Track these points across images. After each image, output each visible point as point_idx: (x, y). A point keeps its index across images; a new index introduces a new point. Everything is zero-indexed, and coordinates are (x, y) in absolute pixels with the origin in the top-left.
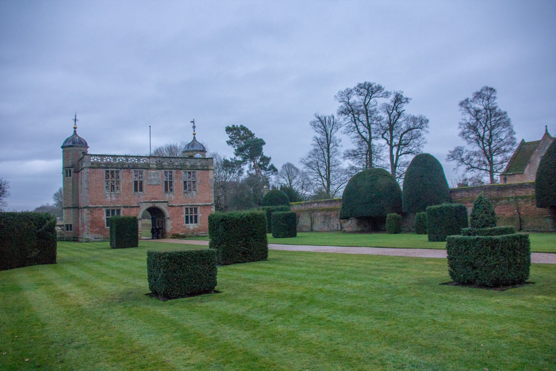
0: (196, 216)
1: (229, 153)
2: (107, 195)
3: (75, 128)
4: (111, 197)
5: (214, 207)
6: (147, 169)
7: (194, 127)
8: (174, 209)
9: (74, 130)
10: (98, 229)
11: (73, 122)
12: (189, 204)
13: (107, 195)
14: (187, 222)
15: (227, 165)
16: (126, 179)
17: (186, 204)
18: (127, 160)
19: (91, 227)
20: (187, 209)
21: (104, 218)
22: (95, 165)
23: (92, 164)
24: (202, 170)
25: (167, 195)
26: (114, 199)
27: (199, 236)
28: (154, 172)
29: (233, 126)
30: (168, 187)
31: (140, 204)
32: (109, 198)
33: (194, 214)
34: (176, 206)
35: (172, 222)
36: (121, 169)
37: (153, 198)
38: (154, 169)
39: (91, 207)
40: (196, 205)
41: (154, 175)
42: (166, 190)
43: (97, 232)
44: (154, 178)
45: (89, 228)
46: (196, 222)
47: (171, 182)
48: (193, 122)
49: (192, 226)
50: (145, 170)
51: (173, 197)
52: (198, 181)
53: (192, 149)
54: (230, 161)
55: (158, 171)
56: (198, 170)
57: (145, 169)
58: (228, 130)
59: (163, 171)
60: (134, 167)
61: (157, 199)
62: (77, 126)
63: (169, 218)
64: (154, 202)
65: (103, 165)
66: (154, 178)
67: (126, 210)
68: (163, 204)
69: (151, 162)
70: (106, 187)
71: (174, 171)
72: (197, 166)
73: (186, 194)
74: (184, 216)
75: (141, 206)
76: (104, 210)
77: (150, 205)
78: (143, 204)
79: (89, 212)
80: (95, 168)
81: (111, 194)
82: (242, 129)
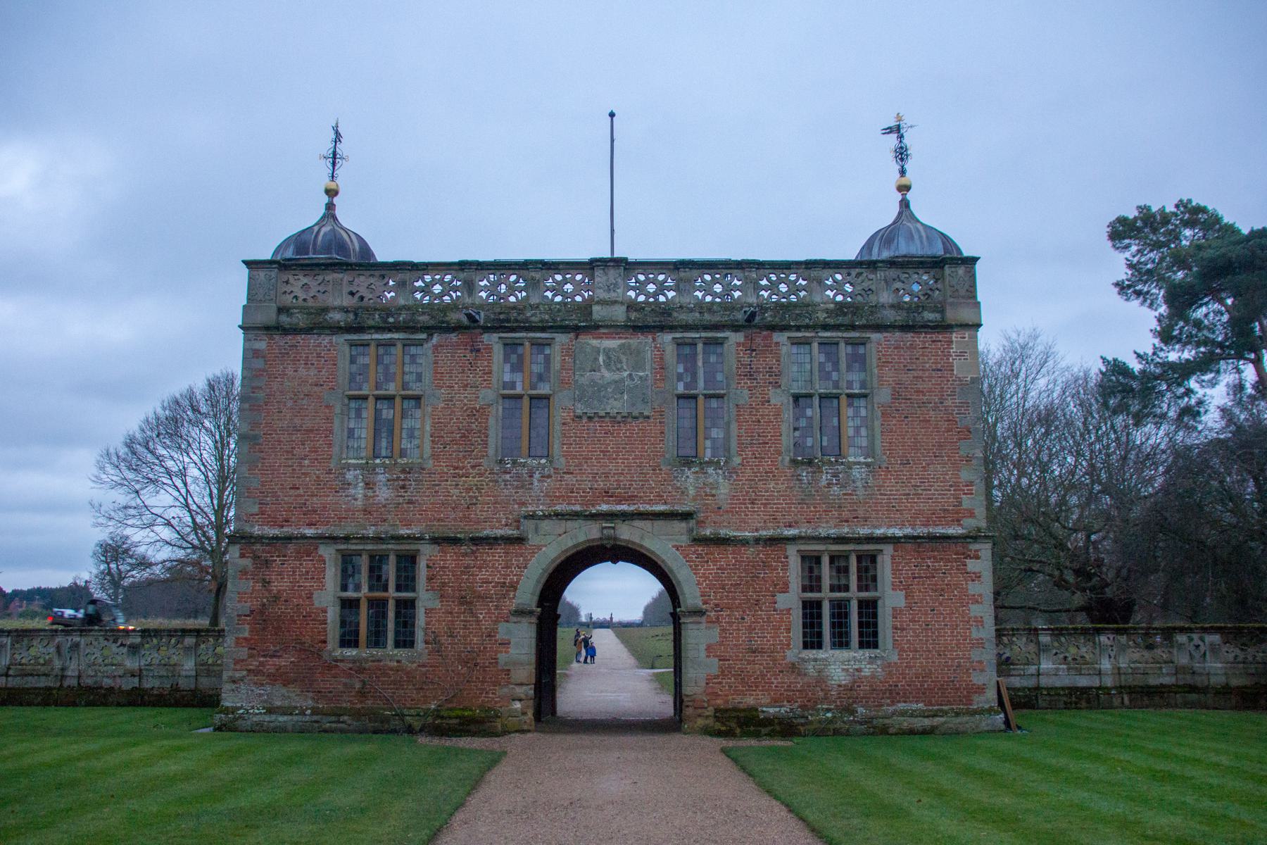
0: (869, 609)
1: (1133, 333)
3: (332, 193)
4: (368, 485)
5: (985, 549)
6: (577, 330)
7: (902, 154)
8: (727, 557)
9: (326, 199)
10: (286, 661)
11: (326, 167)
12: (823, 532)
13: (350, 476)
14: (812, 641)
15: (1124, 389)
17: (804, 530)
18: (470, 287)
19: (251, 645)
20: (811, 562)
21: (327, 597)
22: (299, 319)
23: (281, 310)
24: (905, 328)
25: (689, 479)
26: (384, 494)
27: (884, 731)
28: (612, 344)
29: (1144, 209)
31: (528, 525)
32: (359, 491)
33: (854, 594)
34: (744, 542)
35: (714, 635)
36: (430, 330)
37: (607, 494)
38: (614, 329)
39: (260, 539)
40: (870, 539)
41: (612, 361)
43: (280, 678)
45: (243, 652)
46: (869, 640)
48: (896, 130)
49: (839, 665)
50: (561, 339)
51: (724, 489)
52: (883, 396)
53: (886, 255)
54: (1136, 366)
55: (636, 341)
56: (879, 327)
57: (564, 329)
58: (1121, 231)
59: (667, 337)
60: (506, 322)
61: (631, 499)
62: (341, 182)
63: (700, 613)
65: (336, 316)
67: (451, 558)
69: (601, 294)
71: (735, 338)
72: (876, 308)
73: (804, 474)
74: (791, 600)
75: (533, 540)
76: (328, 552)
78: (546, 525)
79: (247, 562)
80: (295, 331)
81: (368, 469)
82: (1186, 224)
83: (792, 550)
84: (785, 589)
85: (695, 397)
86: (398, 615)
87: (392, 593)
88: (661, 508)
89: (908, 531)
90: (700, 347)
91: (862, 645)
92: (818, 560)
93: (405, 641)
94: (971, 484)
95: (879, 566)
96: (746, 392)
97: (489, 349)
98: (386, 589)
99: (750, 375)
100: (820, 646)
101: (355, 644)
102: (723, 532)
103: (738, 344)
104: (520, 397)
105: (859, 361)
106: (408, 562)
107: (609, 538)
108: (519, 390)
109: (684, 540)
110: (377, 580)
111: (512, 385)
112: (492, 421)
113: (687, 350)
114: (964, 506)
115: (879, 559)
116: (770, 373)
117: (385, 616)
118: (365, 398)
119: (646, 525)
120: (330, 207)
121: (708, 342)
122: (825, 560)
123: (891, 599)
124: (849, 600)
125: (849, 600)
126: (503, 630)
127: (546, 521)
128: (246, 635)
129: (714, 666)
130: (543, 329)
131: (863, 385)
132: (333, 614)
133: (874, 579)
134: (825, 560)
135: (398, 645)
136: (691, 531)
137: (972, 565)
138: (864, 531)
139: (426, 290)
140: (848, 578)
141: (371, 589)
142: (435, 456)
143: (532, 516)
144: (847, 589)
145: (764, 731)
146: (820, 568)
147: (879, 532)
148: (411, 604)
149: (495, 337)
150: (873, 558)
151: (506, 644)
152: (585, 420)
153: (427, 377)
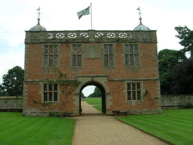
9: (38, 21)
14: (129, 99)
20: (129, 84)
21: (41, 92)
33: (136, 90)
34: (117, 81)
35: (111, 98)
42: (106, 64)
50: (83, 44)
52: (141, 55)
59: (102, 44)
63: (109, 94)
64: (93, 77)
68: (101, 78)
70: (45, 62)
71: (114, 44)
74: (125, 91)
76: (41, 84)
77: (89, 79)
83: (125, 82)
84: (124, 89)
85: (108, 55)
87: (53, 91)
88: (102, 75)
90: (108, 46)
92: (130, 84)
93: (56, 99)
94: (156, 70)
95: (141, 85)
96: (117, 54)
97: (70, 46)
99: (117, 51)
100: (130, 99)
102: (113, 79)
103: (115, 45)
104: (76, 55)
105: (136, 48)
106: (56, 86)
107: (92, 81)
108: (76, 54)
109: (106, 81)
111: (74, 53)
112: (71, 60)
113: (106, 46)
114: (155, 74)
115: (141, 84)
116: (121, 50)
118: (47, 55)
119: (99, 78)
120: (39, 22)
121: (110, 45)
122: (131, 84)
124: (135, 91)
125: (135, 91)
126: (74, 98)
127: (81, 78)
128: (27, 99)
129: (111, 103)
130: (80, 43)
131: (137, 53)
132: (43, 95)
133: (140, 87)
134: (131, 84)
135: (54, 100)
136: (107, 79)
137: (157, 85)
138: (138, 79)
139: (58, 36)
140: (135, 87)
141: (49, 90)
142: (61, 66)
143: (79, 77)
145: (121, 114)
146: (130, 86)
147: (141, 79)
148: (56, 93)
150: (140, 84)
151: (74, 100)
152: (88, 59)
153: (59, 52)
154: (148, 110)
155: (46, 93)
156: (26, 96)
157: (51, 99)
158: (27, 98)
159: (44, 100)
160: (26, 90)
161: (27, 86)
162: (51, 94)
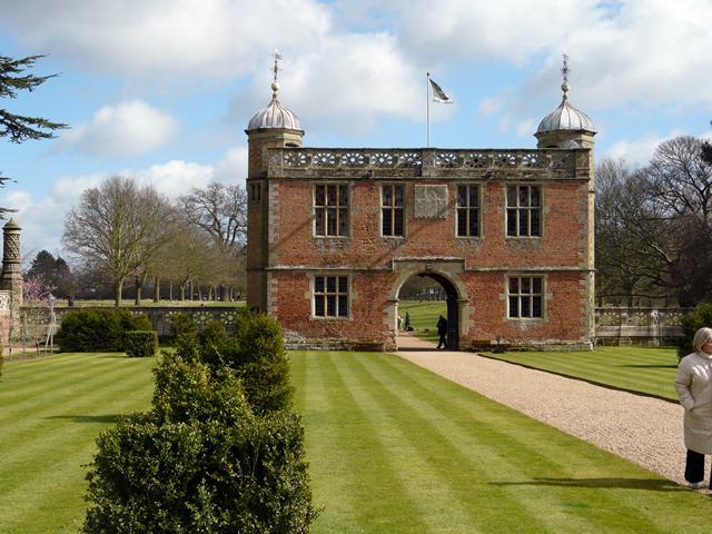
0: (538, 300)
2: (318, 243)
14: (514, 313)
16: (369, 206)
18: (366, 160)
20: (513, 282)
30: (470, 224)
40: (536, 272)
44: (434, 201)
46: (538, 313)
47: (475, 213)
52: (546, 210)
64: (430, 261)
66: (434, 201)
68: (450, 264)
86: (340, 302)
87: (337, 293)
88: (452, 258)
89: (555, 268)
91: (534, 316)
92: (517, 280)
98: (334, 291)
101: (322, 314)
106: (344, 280)
110: (332, 288)
117: (334, 302)
123: (547, 297)
138: (535, 269)
144: (528, 292)
147: (542, 269)
149: (380, 183)
150: (540, 279)
154: (558, 341)
155: (323, 297)
156: (273, 305)
157: (332, 312)
158: (276, 309)
159: (317, 314)
160: (276, 290)
161: (275, 281)
162: (332, 300)
